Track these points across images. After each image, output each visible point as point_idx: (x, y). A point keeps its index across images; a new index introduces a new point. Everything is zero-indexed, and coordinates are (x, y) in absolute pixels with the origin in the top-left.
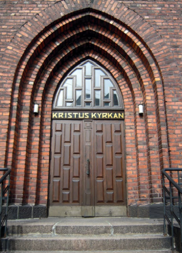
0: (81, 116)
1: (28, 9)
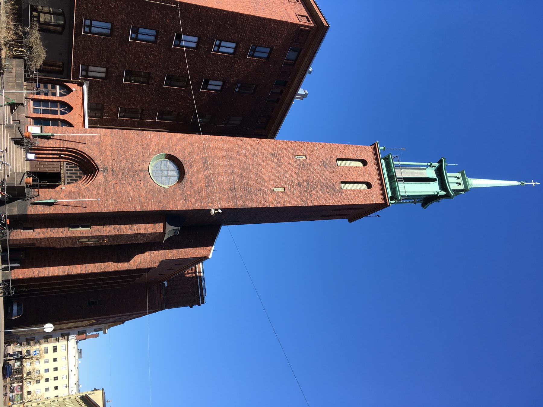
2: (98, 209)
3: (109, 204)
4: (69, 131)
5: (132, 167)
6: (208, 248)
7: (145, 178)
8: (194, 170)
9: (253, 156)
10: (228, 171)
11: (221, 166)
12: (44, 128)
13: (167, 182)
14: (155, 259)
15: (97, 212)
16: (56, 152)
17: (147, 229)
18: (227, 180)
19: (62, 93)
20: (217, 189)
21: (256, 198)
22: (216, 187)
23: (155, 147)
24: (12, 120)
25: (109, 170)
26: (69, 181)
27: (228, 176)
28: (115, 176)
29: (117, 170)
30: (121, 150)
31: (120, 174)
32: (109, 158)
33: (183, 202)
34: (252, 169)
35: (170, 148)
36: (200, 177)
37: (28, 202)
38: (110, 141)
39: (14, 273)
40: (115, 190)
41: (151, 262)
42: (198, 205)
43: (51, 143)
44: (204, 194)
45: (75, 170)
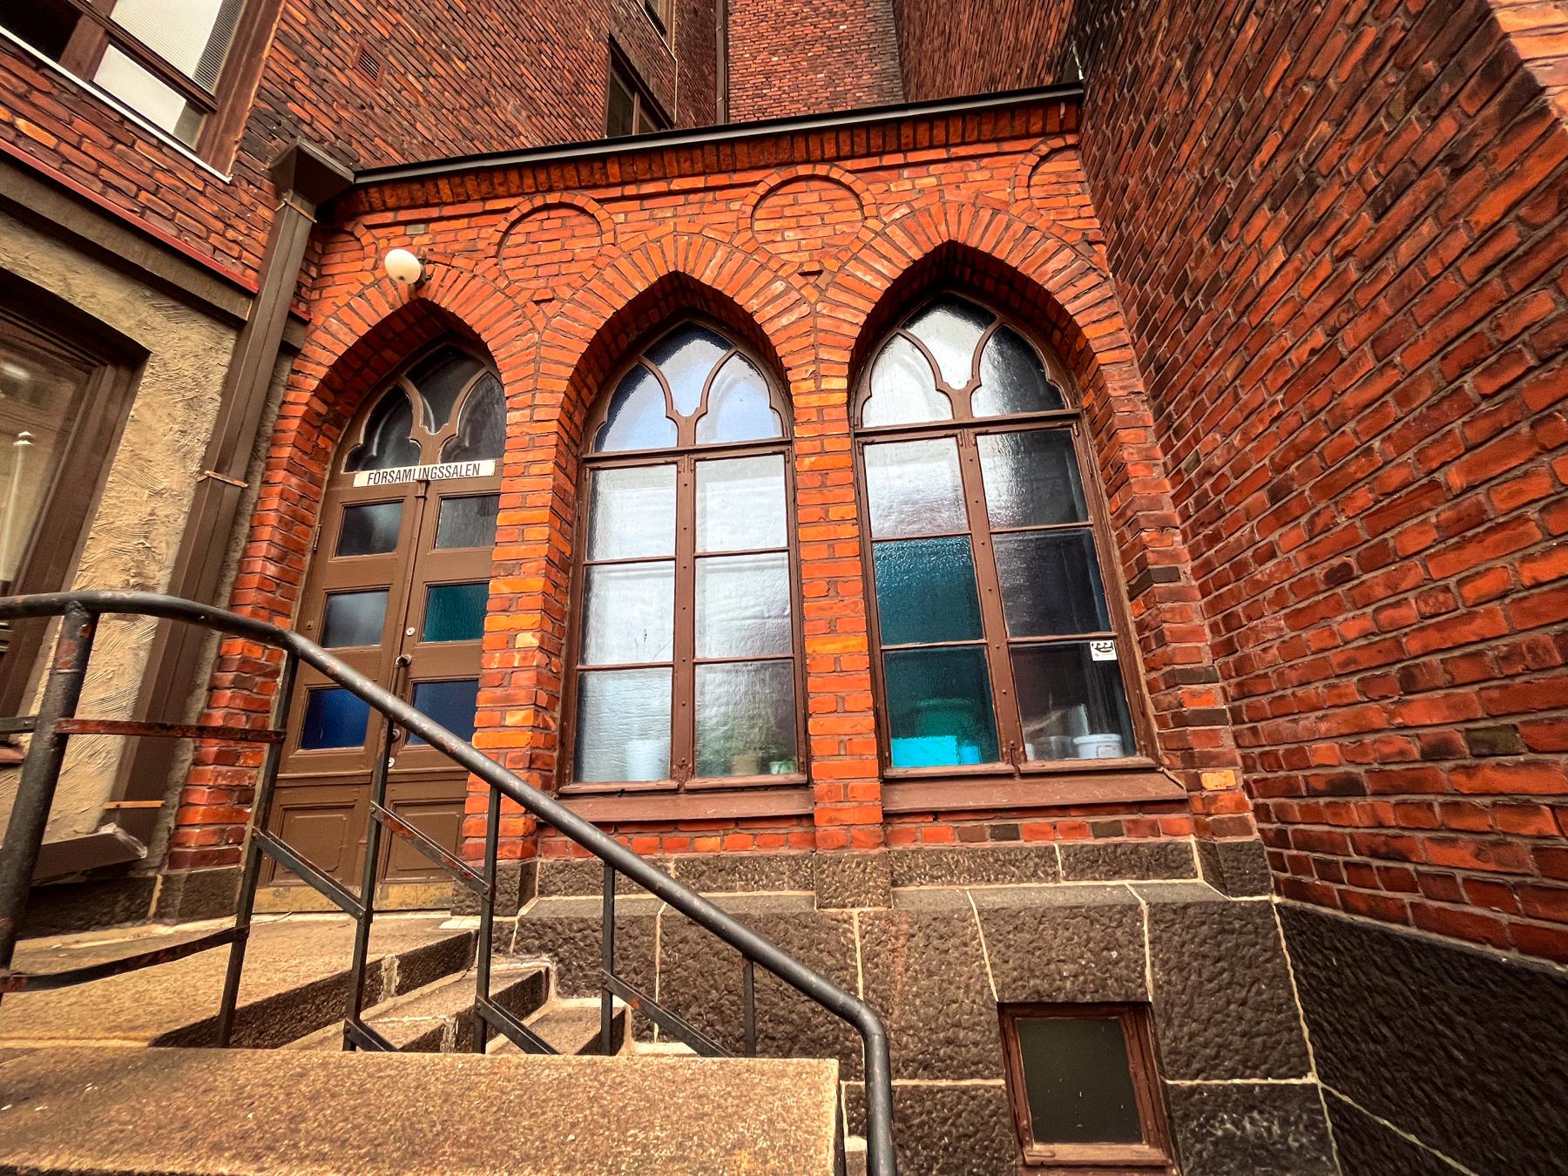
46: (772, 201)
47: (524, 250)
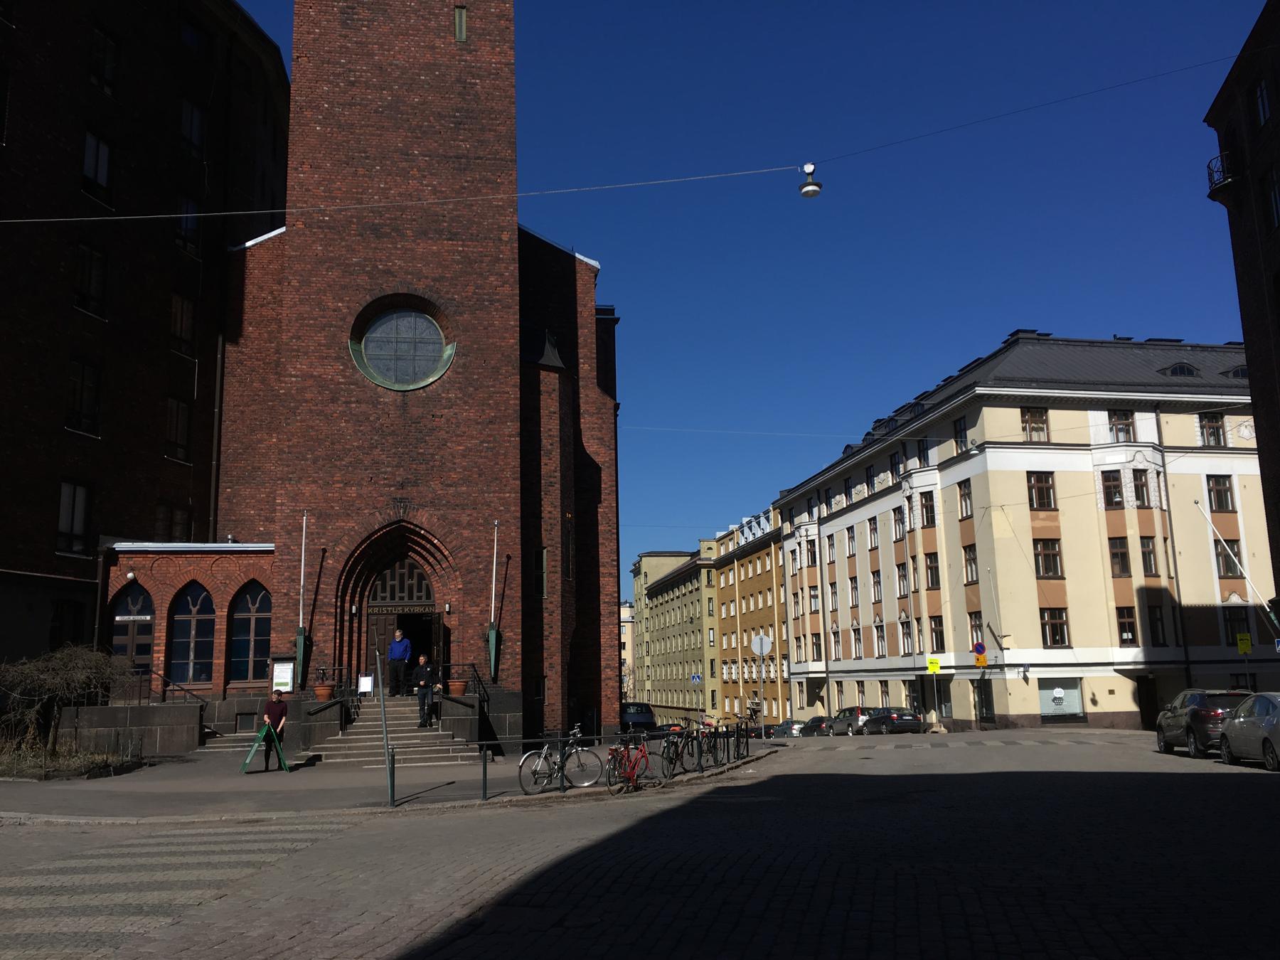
0: (395, 610)
1: (344, 522)
2: (513, 528)
3: (500, 499)
4: (285, 591)
5: (393, 433)
6: (578, 268)
7: (427, 404)
8: (400, 267)
9: (352, 84)
10: (403, 169)
11: (387, 186)
12: (277, 653)
13: (431, 347)
14: (593, 403)
15: (520, 530)
16: (347, 624)
17: (550, 412)
18: (431, 175)
19: (139, 607)
20: (459, 210)
21: (486, 98)
22: (452, 210)
23: (329, 367)
24: (235, 733)
25: (402, 494)
26: (423, 594)
27: (418, 171)
28: (420, 479)
29: (401, 475)
30: (343, 460)
31: (415, 466)
32: (364, 491)
33: (496, 310)
34: (394, 92)
35: (331, 326)
36: (423, 252)
37: (491, 691)
38: (314, 487)
39: (607, 720)
40: (461, 482)
41: (602, 414)
42: (506, 268)
43: (324, 636)
44: (475, 250)
45: (393, 579)
46: (217, 562)
47: (158, 569)
